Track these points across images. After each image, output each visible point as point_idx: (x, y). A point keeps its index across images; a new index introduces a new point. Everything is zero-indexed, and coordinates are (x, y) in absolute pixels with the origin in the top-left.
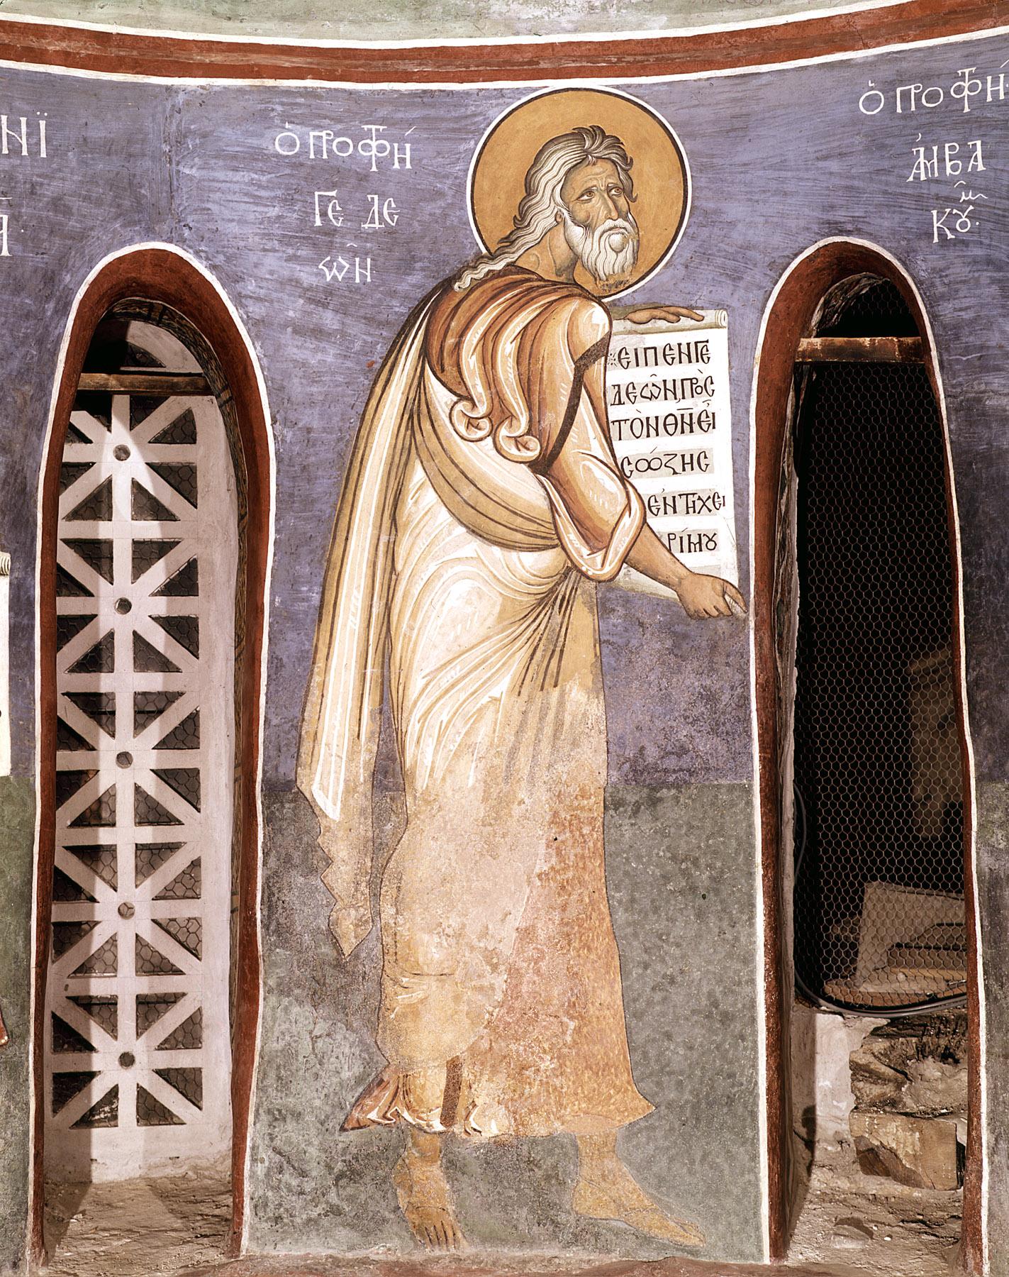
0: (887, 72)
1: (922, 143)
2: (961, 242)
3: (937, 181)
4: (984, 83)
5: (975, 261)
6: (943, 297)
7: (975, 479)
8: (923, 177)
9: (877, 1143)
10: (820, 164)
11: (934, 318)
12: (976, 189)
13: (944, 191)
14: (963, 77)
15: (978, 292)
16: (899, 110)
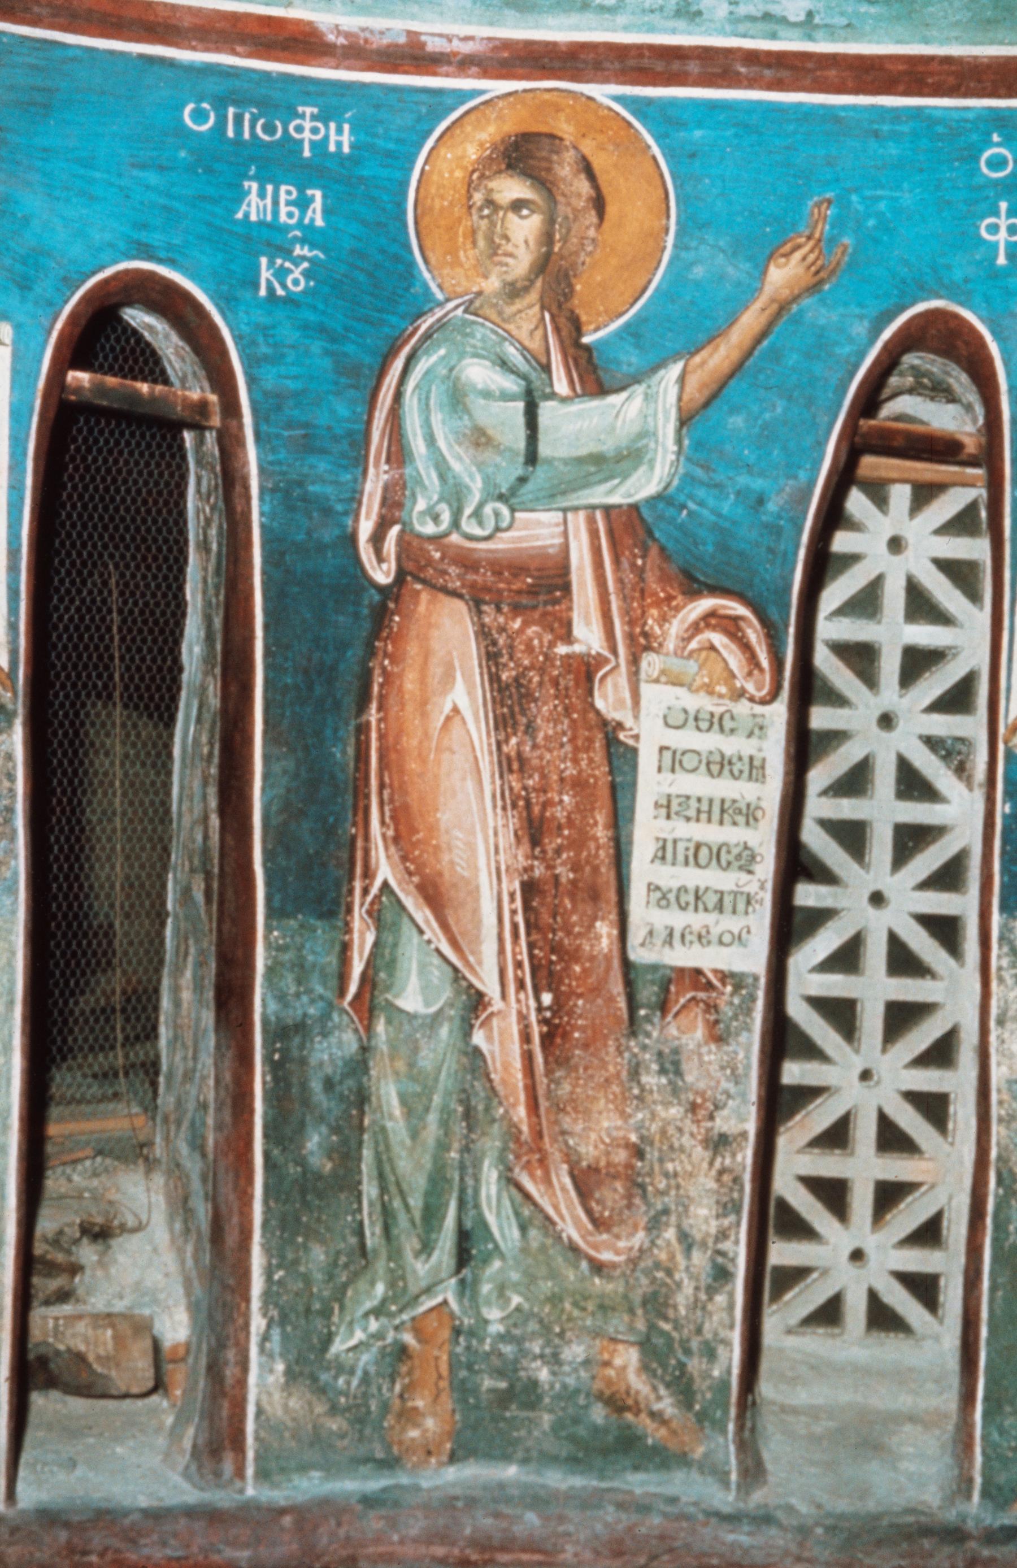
0: (213, 86)
1: (255, 178)
2: (290, 301)
3: (269, 226)
4: (327, 128)
5: (305, 327)
6: (266, 358)
7: (287, 571)
8: (253, 218)
9: (62, 1347)
10: (135, 172)
11: (252, 381)
12: (313, 246)
13: (278, 239)
14: (303, 116)
15: (308, 362)
16: (230, 133)
